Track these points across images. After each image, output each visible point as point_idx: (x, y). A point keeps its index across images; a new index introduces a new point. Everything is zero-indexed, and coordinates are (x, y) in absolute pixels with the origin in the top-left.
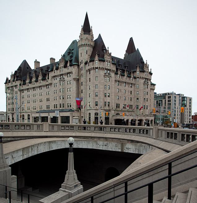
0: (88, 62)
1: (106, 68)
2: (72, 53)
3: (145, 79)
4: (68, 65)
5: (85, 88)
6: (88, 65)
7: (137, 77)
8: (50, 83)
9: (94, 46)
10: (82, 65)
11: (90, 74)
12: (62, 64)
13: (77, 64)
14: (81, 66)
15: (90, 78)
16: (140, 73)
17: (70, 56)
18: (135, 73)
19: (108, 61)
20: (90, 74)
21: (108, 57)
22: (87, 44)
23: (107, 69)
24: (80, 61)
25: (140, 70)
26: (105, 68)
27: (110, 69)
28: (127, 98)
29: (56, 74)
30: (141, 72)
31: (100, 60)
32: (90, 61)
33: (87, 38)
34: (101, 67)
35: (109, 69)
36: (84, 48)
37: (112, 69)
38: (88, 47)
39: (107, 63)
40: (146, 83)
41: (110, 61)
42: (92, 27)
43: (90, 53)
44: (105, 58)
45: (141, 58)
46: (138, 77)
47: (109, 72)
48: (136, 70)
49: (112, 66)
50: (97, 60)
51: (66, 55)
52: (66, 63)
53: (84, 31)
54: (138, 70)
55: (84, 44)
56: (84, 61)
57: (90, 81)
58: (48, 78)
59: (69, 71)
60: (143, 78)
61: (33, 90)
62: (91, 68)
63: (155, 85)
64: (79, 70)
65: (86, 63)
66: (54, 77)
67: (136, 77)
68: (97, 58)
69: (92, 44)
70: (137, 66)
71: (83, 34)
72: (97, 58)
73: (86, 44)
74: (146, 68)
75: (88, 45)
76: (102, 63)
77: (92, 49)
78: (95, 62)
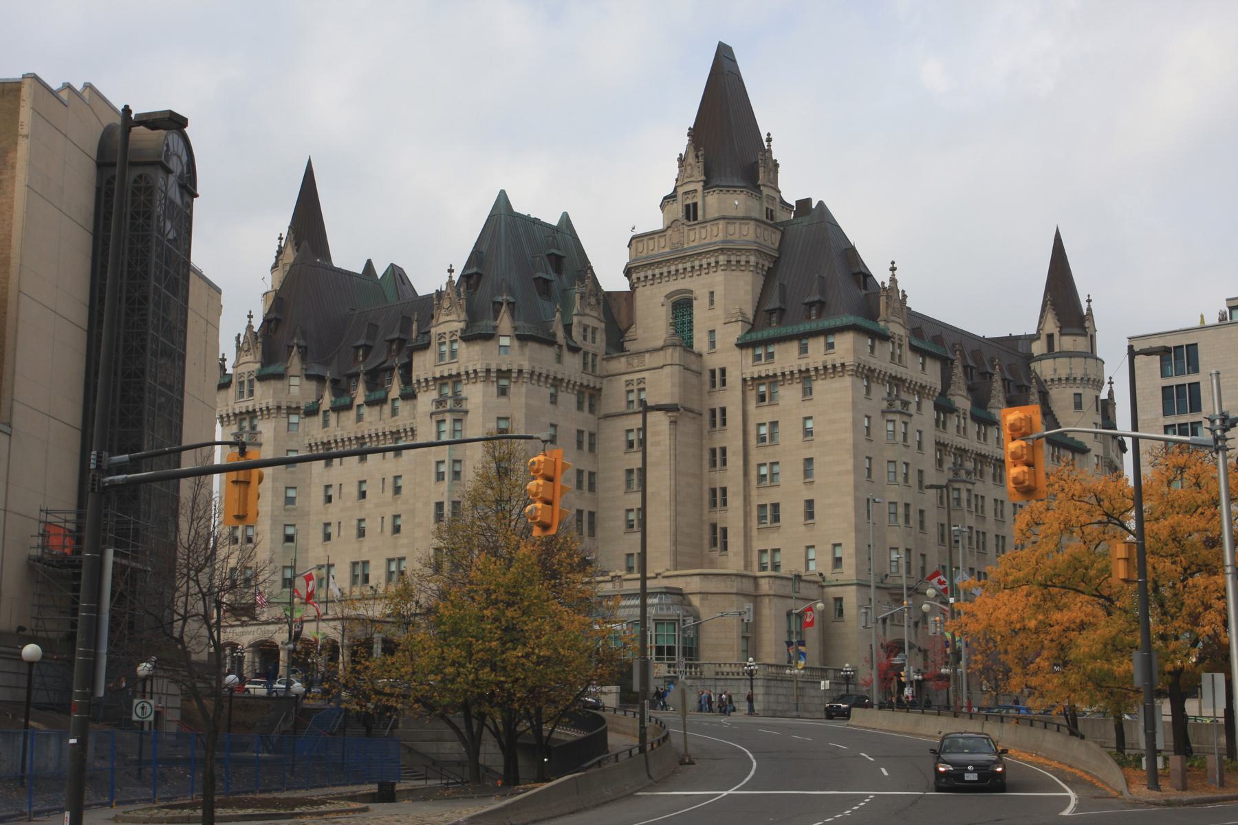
27: (251, 409)
28: (370, 526)
70: (500, 299)
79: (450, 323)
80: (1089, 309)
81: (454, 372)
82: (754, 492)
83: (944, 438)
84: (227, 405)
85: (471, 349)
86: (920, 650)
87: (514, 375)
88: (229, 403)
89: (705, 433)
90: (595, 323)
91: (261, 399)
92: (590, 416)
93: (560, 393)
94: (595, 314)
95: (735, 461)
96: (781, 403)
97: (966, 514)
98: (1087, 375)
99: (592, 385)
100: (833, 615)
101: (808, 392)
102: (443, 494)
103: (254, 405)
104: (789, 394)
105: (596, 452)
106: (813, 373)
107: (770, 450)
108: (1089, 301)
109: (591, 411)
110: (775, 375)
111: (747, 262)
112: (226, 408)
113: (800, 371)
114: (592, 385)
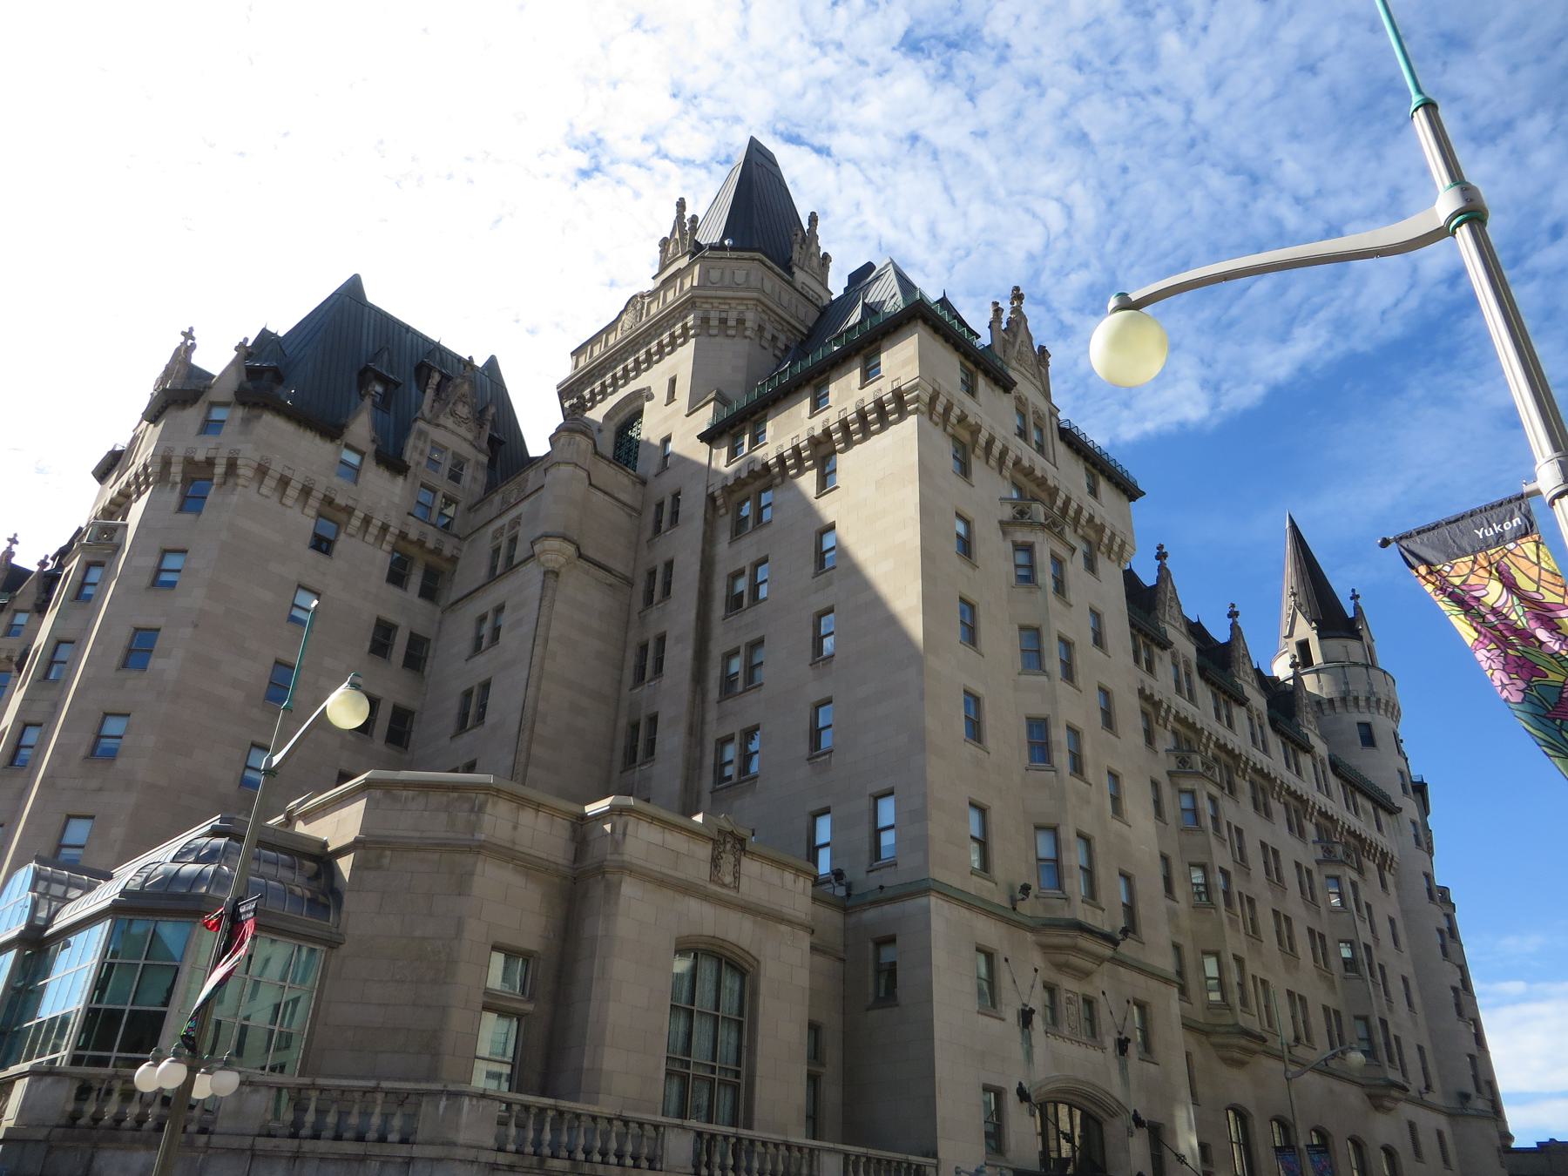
80: (1357, 608)
82: (712, 714)
83: (1151, 688)
86: (1138, 1122)
87: (219, 470)
89: (635, 617)
90: (466, 450)
92: (421, 603)
93: (342, 536)
94: (462, 431)
95: (679, 656)
97: (1213, 841)
98: (1374, 693)
100: (871, 989)
105: (426, 673)
108: (1355, 597)
109: (429, 592)
110: (766, 467)
111: (741, 322)
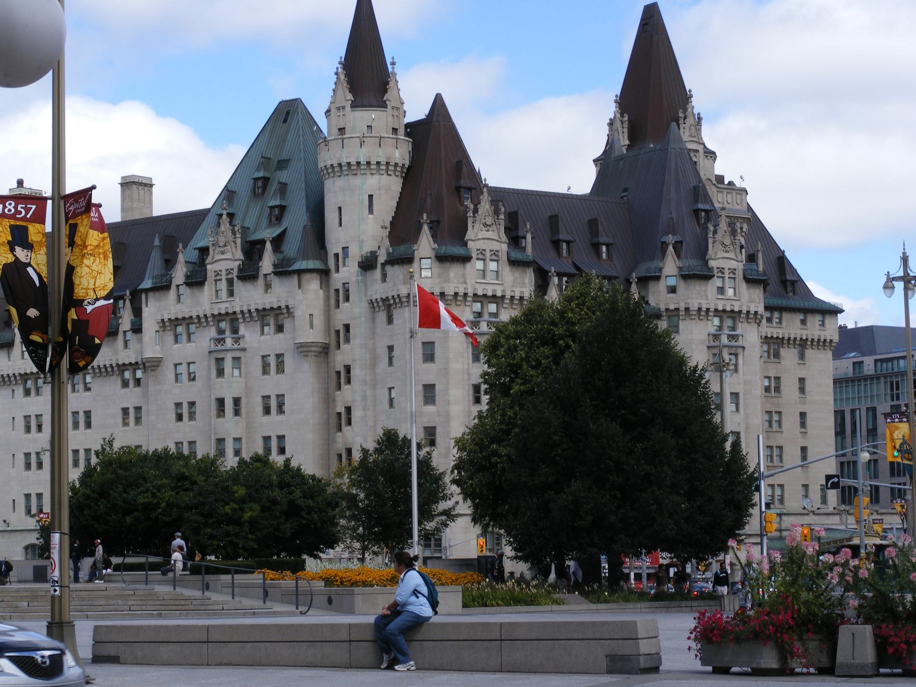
0: (382, 258)
1: (475, 295)
2: (283, 188)
3: (721, 313)
4: (267, 263)
5: (365, 398)
6: (378, 272)
7: (667, 310)
8: (150, 360)
9: (407, 164)
10: (348, 273)
11: (390, 320)
12: (229, 256)
13: (317, 264)
14: (338, 279)
15: (391, 348)
16: (682, 282)
17: (272, 208)
18: (652, 284)
19: (488, 254)
20: (390, 320)
21: (490, 234)
22: (373, 162)
23: (485, 296)
24: (334, 246)
25: (680, 269)
26: (471, 294)
27: (499, 294)
29: (185, 309)
30: (689, 281)
31: (442, 259)
32: (392, 261)
33: (370, 127)
34: (450, 291)
35: (494, 296)
36: (356, 181)
37: (508, 294)
38: (376, 177)
39: (479, 265)
40: (724, 340)
41: (495, 253)
42: (393, 64)
43: (386, 207)
44: (471, 245)
45: (693, 183)
46: (672, 307)
47: (492, 308)
48: (661, 270)
49: (508, 274)
50: (430, 253)
51: (244, 191)
52: (253, 250)
53: (351, 91)
54: (670, 266)
55: (353, 161)
56: (356, 254)
57: (391, 363)
58: (137, 329)
59: (269, 300)
60: (703, 313)
61: (20, 390)
62: (395, 294)
63: (841, 311)
64: (327, 299)
65: (368, 264)
66: (175, 322)
67: (663, 308)
68: (425, 245)
69: (401, 154)
71: (348, 108)
72: (425, 245)
73: (368, 163)
74: (721, 254)
75: (378, 163)
76: (455, 271)
77: (395, 184)
78: (416, 265)
79: (729, 260)
81: (736, 309)
84: (465, 283)
85: (752, 291)
88: (468, 281)
91: (513, 286)
96: (783, 362)
99: (775, 336)
101: (802, 356)
102: (739, 425)
103: (504, 291)
104: (789, 355)
106: (809, 343)
107: (776, 400)
112: (464, 286)
113: (801, 339)
114: (775, 336)
